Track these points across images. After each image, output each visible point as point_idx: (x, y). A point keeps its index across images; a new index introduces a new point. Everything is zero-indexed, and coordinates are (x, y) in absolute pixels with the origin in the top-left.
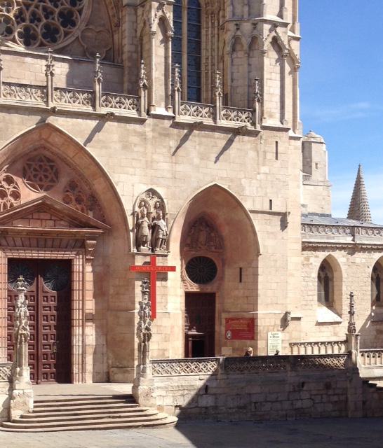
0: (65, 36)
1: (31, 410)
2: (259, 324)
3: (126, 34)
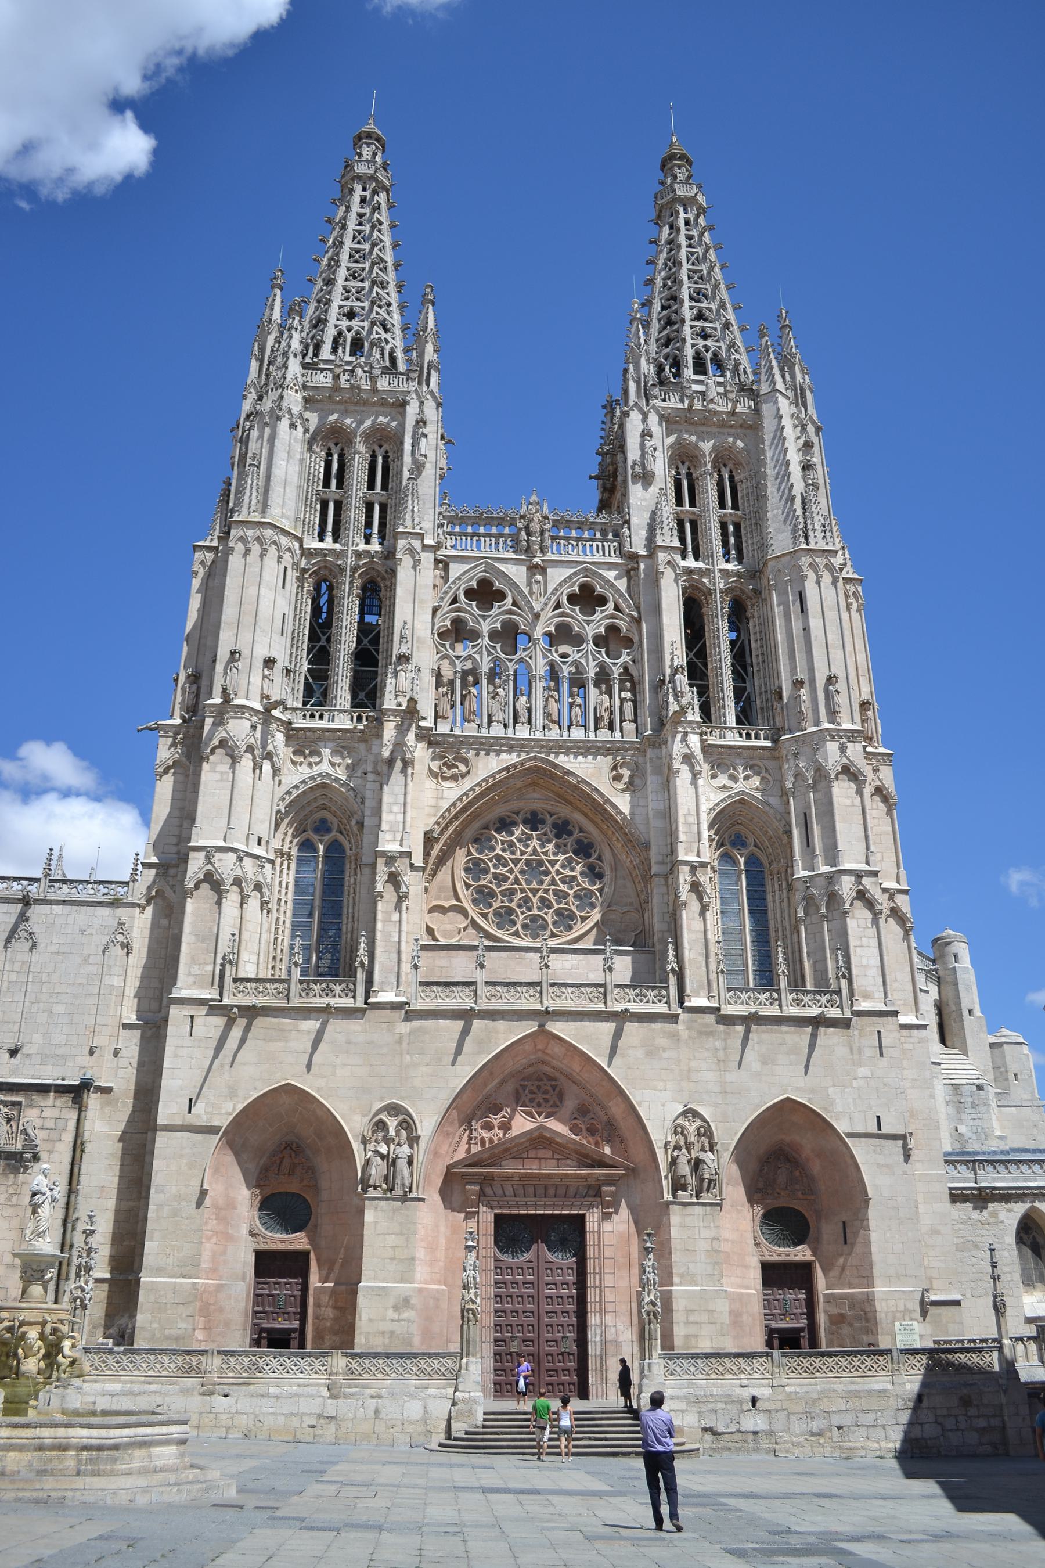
1: (480, 1422)
2: (878, 1309)
3: (655, 911)
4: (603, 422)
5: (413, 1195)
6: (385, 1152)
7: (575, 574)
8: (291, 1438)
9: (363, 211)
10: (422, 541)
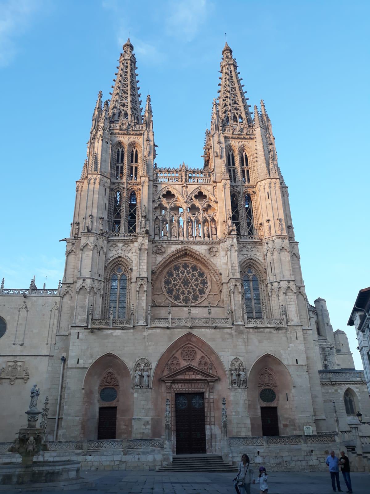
0: (201, 298)
1: (171, 462)
3: (224, 294)
4: (205, 138)
5: (149, 388)
6: (140, 374)
7: (197, 188)
8: (111, 469)
9: (127, 71)
10: (149, 179)
